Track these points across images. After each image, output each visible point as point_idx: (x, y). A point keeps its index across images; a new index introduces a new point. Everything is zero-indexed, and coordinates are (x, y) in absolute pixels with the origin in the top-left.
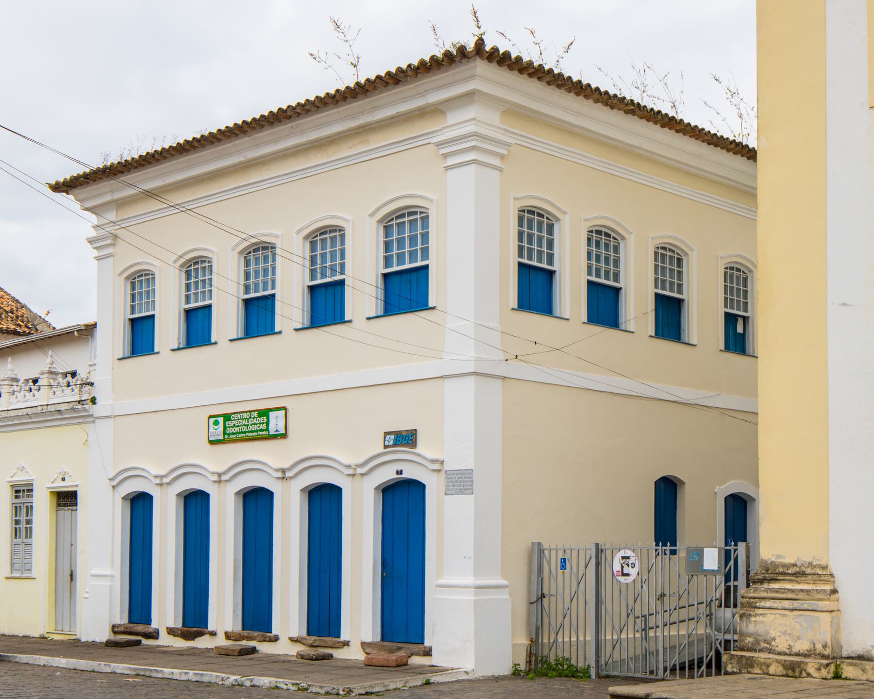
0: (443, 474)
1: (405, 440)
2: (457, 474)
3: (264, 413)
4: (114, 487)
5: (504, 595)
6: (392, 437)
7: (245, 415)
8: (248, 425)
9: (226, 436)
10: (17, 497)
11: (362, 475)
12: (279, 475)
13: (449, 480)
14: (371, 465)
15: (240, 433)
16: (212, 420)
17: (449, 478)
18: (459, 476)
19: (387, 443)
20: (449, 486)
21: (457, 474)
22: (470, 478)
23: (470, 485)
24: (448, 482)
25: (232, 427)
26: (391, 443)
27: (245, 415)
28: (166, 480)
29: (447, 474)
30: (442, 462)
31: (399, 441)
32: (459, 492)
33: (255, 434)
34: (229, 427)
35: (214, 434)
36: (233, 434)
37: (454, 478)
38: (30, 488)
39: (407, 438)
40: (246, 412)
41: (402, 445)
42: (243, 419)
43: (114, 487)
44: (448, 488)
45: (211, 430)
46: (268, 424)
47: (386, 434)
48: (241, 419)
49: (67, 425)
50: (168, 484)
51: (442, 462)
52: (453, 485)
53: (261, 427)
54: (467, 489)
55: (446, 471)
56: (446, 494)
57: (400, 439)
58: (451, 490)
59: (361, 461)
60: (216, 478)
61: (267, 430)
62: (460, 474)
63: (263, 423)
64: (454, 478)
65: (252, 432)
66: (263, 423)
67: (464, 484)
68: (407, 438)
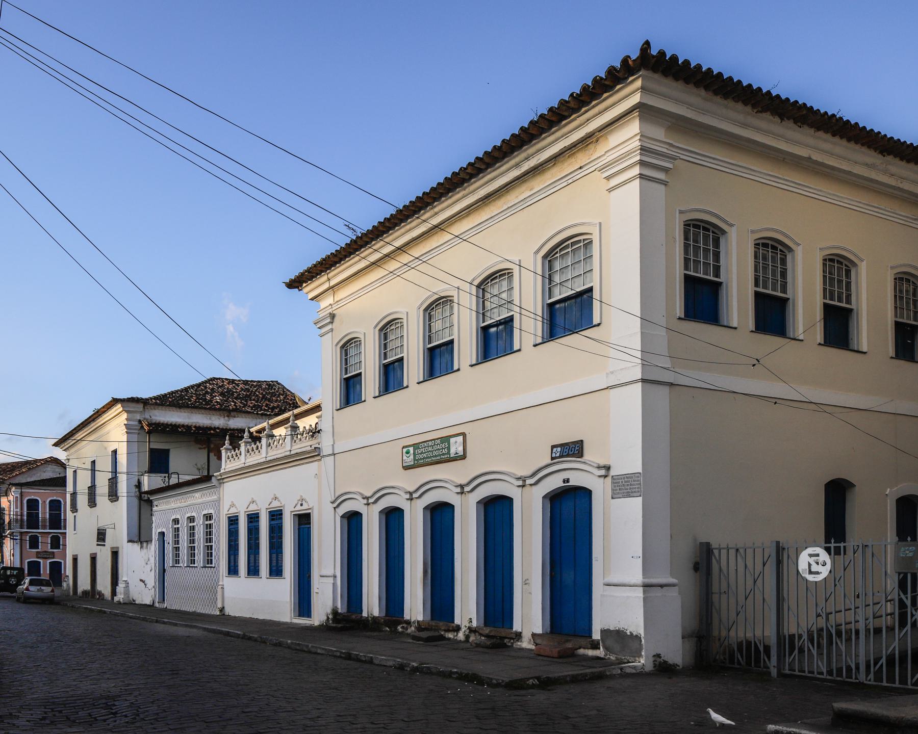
0: (609, 479)
1: (571, 451)
2: (624, 478)
3: (446, 439)
4: (335, 508)
5: (673, 593)
6: (559, 449)
7: (430, 443)
8: (432, 451)
9: (416, 462)
10: (273, 520)
11: (531, 485)
12: (459, 490)
13: (616, 485)
14: (538, 476)
15: (426, 458)
16: (405, 450)
17: (616, 483)
18: (626, 480)
19: (554, 455)
20: (616, 490)
21: (624, 478)
22: (638, 481)
23: (638, 488)
24: (615, 486)
25: (420, 454)
26: (558, 455)
27: (430, 443)
28: (371, 501)
29: (614, 479)
30: (608, 468)
31: (566, 452)
32: (627, 495)
33: (439, 458)
34: (418, 454)
35: (407, 461)
36: (421, 459)
37: (621, 482)
38: (280, 512)
39: (573, 449)
40: (431, 440)
41: (568, 455)
42: (429, 447)
43: (335, 508)
44: (615, 492)
45: (405, 458)
46: (449, 448)
47: (553, 447)
48: (427, 447)
49: (303, 464)
50: (373, 503)
51: (608, 468)
52: (620, 489)
53: (444, 452)
54: (635, 492)
55: (612, 476)
56: (612, 498)
57: (567, 450)
58: (618, 493)
59: (529, 473)
60: (408, 496)
61: (449, 453)
62: (627, 478)
63: (444, 448)
64: (621, 482)
65: (436, 456)
66: (444, 448)
67: (632, 487)
68: (573, 449)
